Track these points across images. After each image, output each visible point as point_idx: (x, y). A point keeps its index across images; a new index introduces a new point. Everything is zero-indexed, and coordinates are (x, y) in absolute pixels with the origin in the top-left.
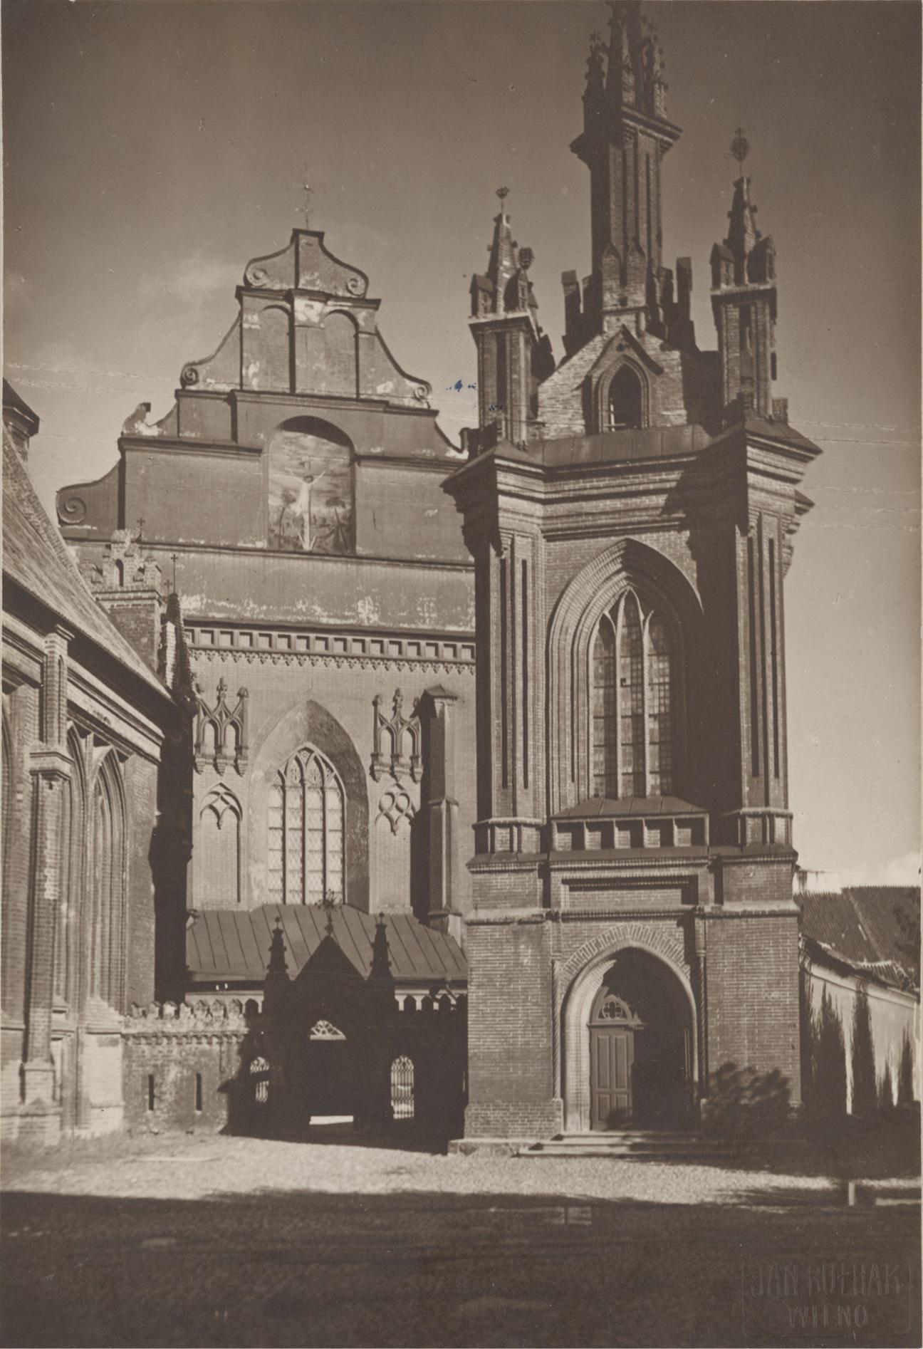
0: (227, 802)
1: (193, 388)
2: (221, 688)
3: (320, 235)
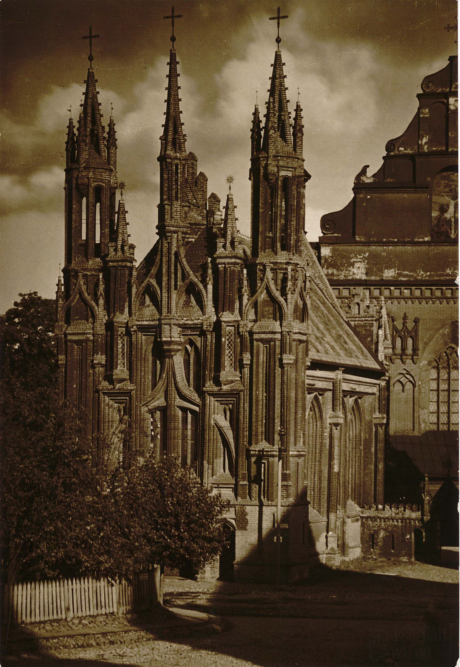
0: (407, 378)
2: (405, 318)
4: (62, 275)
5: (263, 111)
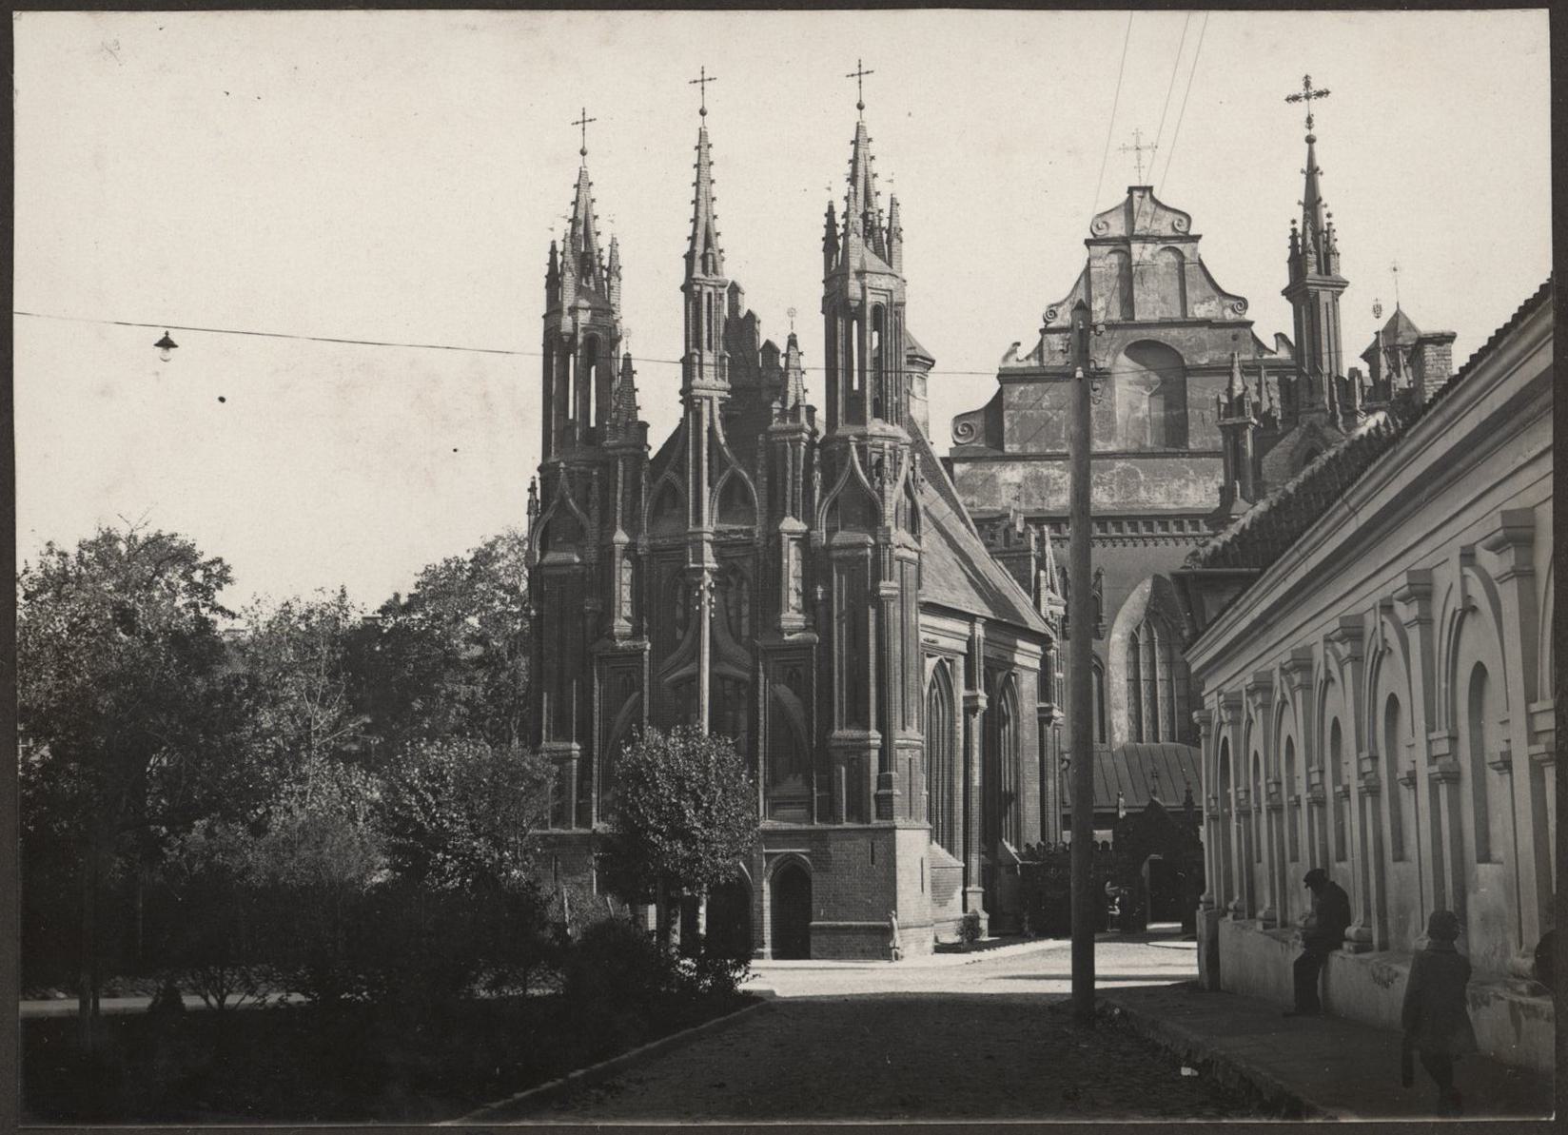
1: (1051, 325)
3: (1150, 189)
4: (538, 475)
5: (840, 208)
